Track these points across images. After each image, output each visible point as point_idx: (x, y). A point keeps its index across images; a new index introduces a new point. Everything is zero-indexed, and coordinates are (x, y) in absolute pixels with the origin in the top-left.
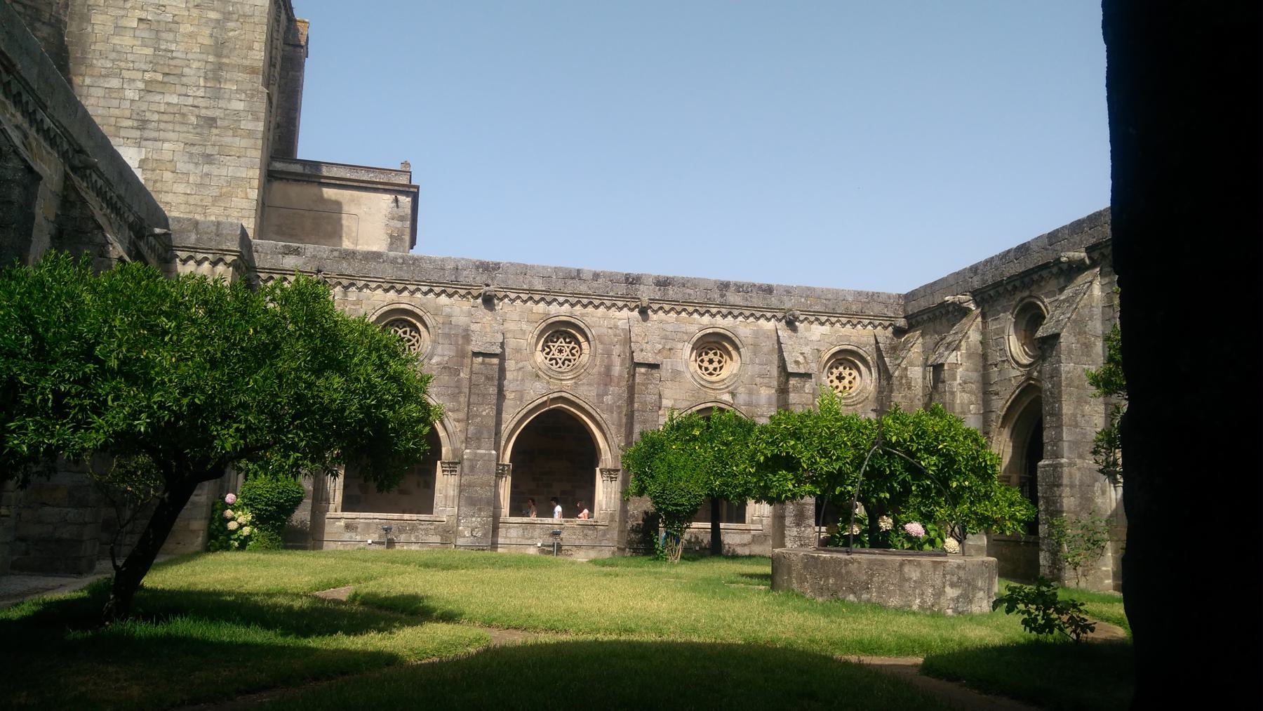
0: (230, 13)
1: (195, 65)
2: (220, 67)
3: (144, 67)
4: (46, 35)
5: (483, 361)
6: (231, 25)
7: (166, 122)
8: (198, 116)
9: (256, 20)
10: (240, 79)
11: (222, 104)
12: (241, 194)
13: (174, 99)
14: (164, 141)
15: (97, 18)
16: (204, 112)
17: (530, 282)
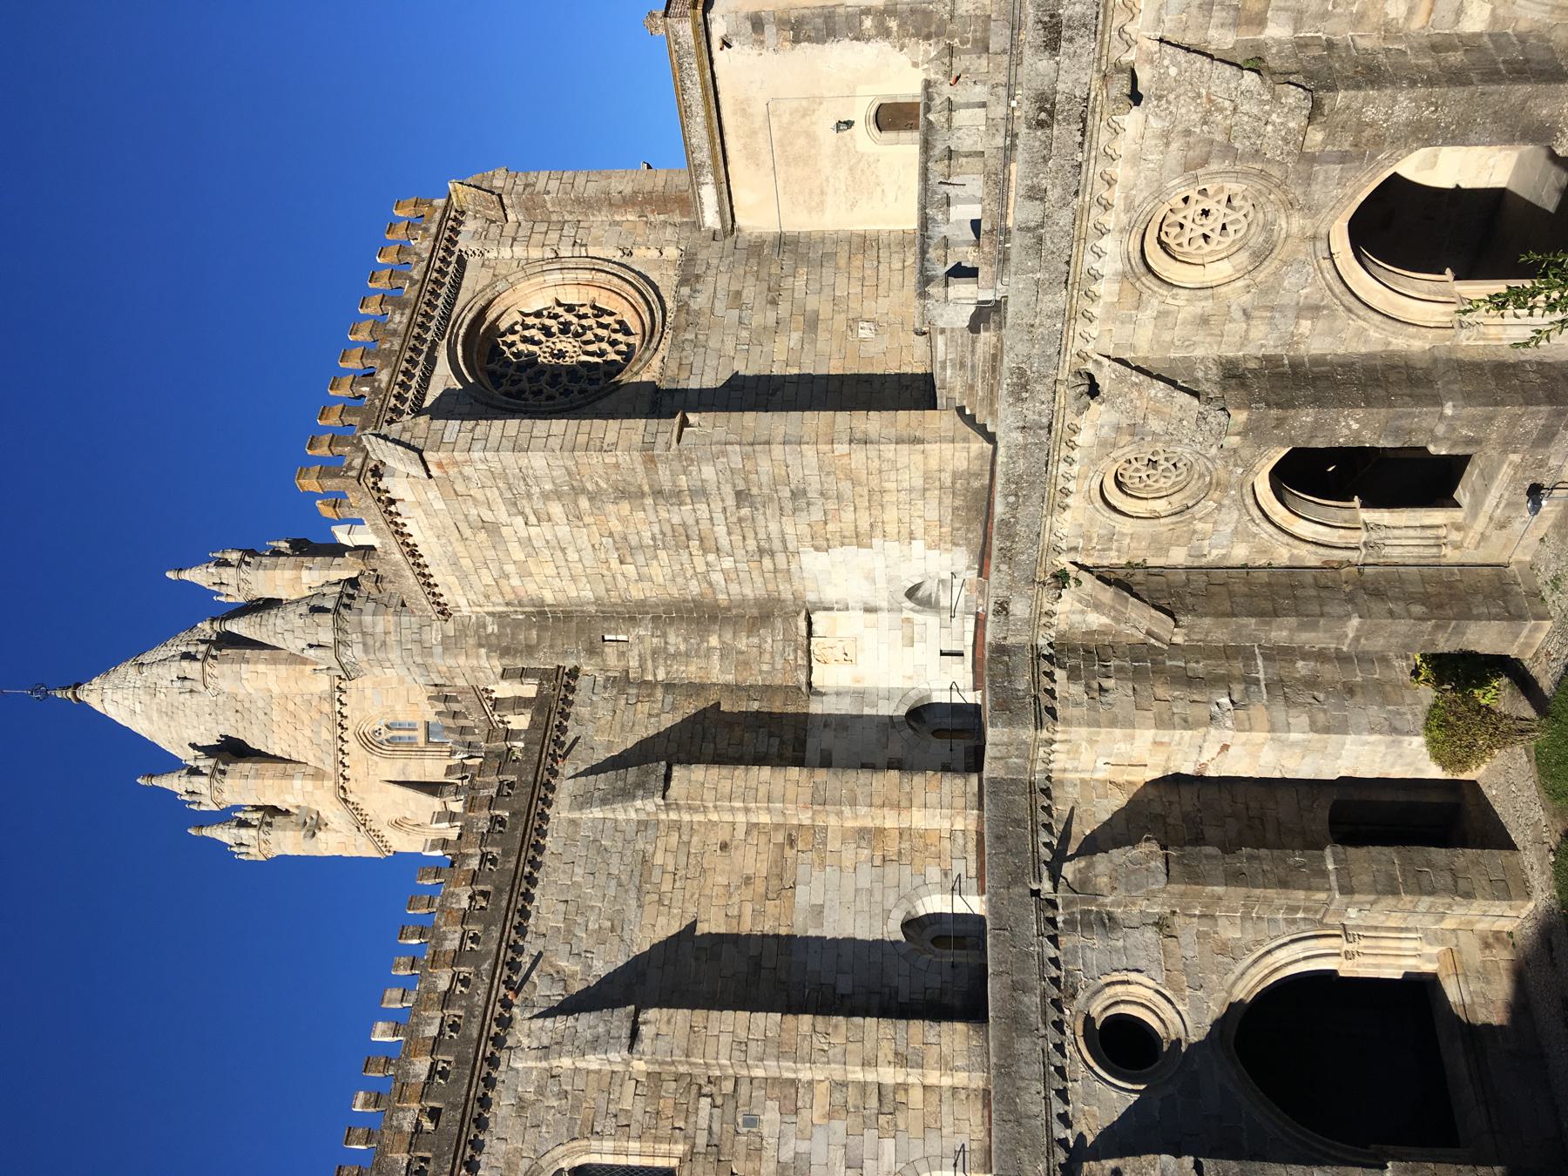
0: (573, 488)
1: (664, 515)
2: (658, 493)
3: (685, 556)
4: (680, 639)
5: (1239, 434)
6: (590, 486)
7: (756, 534)
8: (738, 507)
9: (570, 463)
10: (668, 472)
11: (711, 487)
12: (845, 460)
13: (721, 530)
14: (783, 533)
15: (636, 593)
16: (731, 501)
17: (1049, 317)
